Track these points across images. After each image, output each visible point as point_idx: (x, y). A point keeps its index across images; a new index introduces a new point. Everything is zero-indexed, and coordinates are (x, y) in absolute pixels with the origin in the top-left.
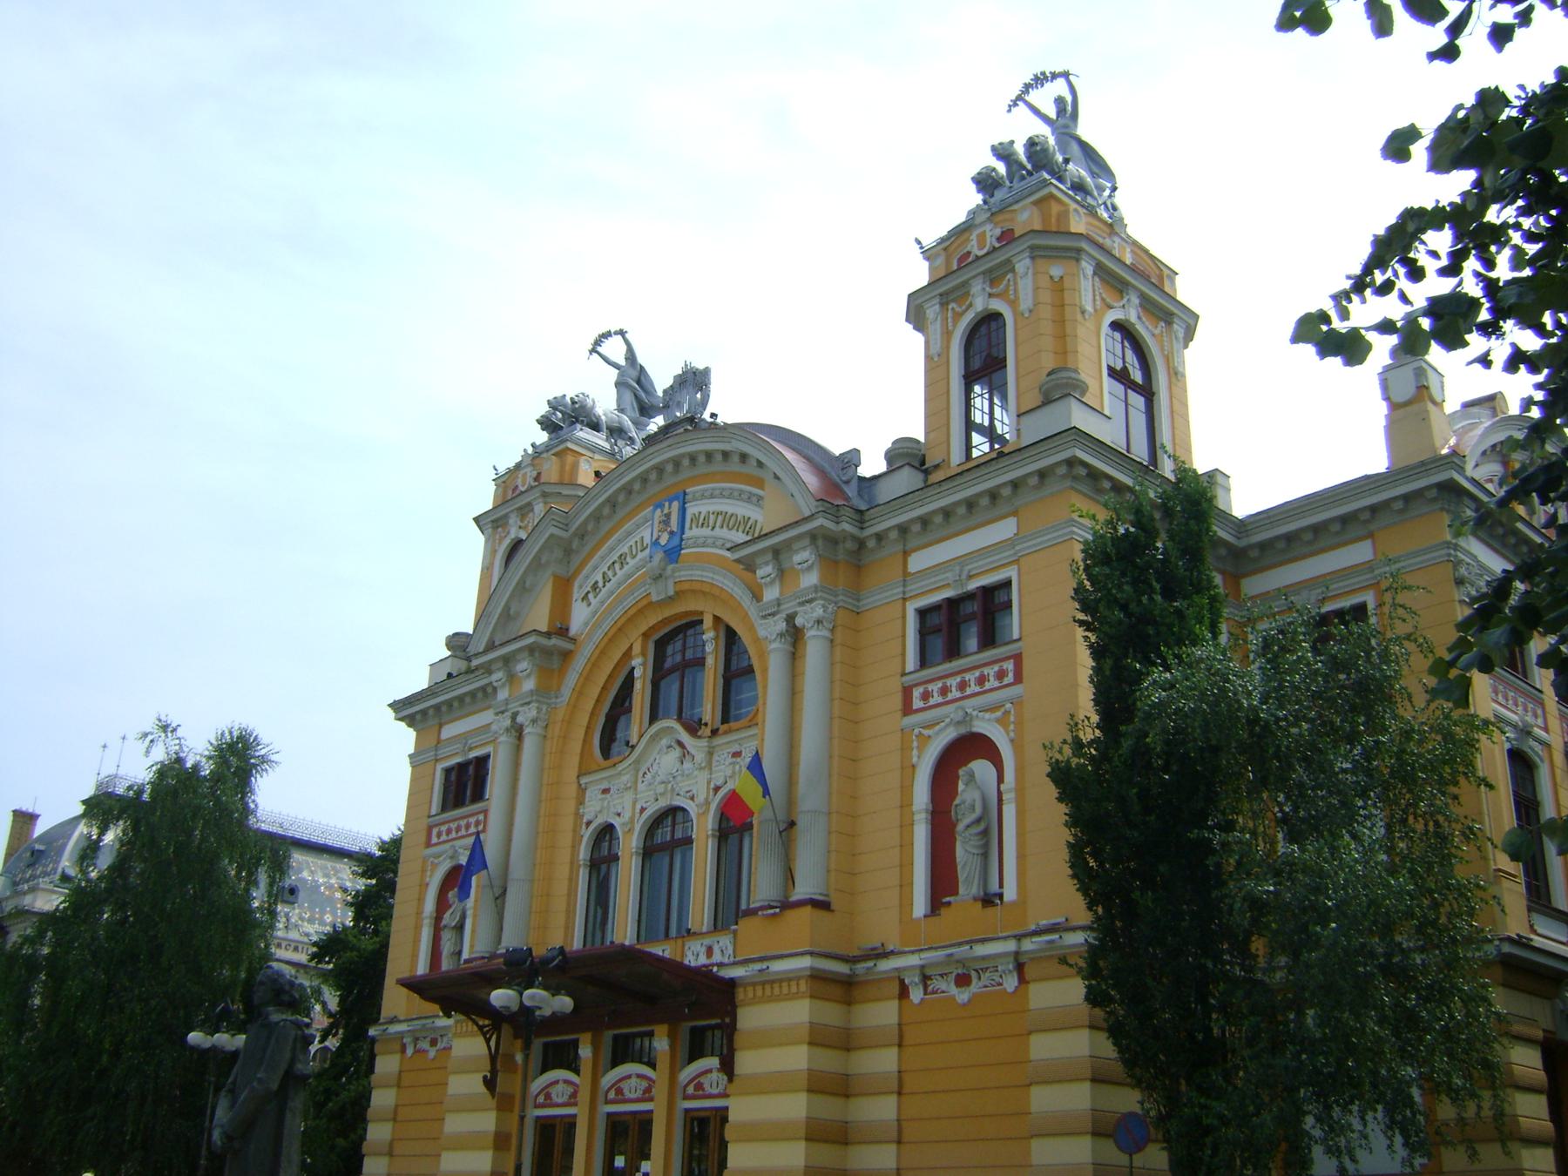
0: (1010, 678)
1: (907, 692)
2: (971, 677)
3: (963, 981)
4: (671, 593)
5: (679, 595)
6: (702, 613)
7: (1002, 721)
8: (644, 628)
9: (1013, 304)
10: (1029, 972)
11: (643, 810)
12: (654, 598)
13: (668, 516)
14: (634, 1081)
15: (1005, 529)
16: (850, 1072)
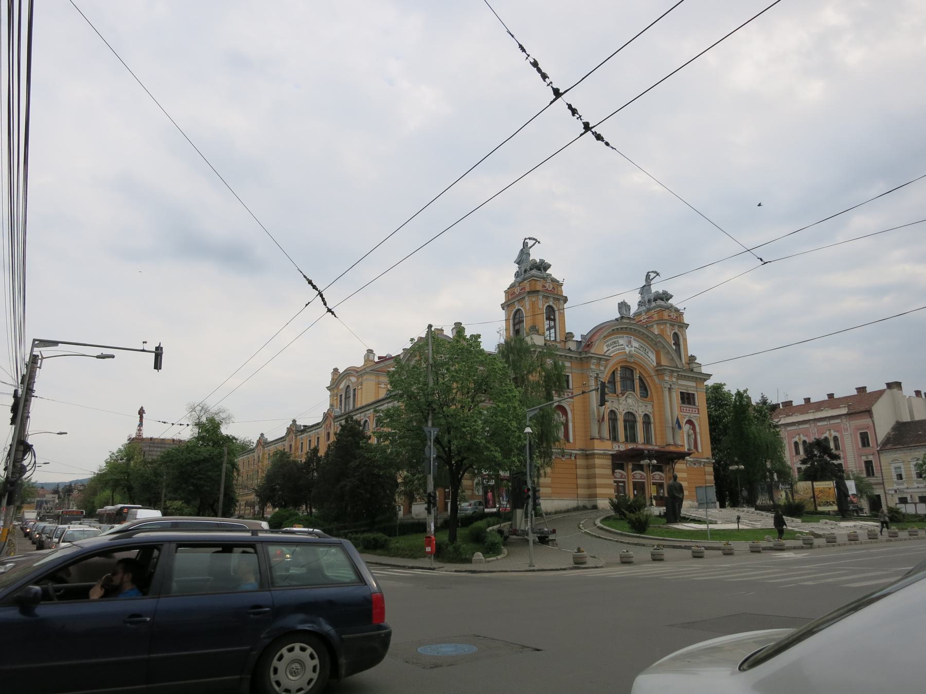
0: (697, 412)
1: (681, 407)
2: (691, 409)
3: (695, 464)
4: (632, 361)
5: (634, 362)
6: (636, 369)
7: (697, 420)
8: (621, 365)
9: (682, 335)
10: (706, 465)
11: (624, 410)
12: (628, 360)
13: (630, 341)
14: (638, 474)
15: (694, 384)
16: (586, 470)
